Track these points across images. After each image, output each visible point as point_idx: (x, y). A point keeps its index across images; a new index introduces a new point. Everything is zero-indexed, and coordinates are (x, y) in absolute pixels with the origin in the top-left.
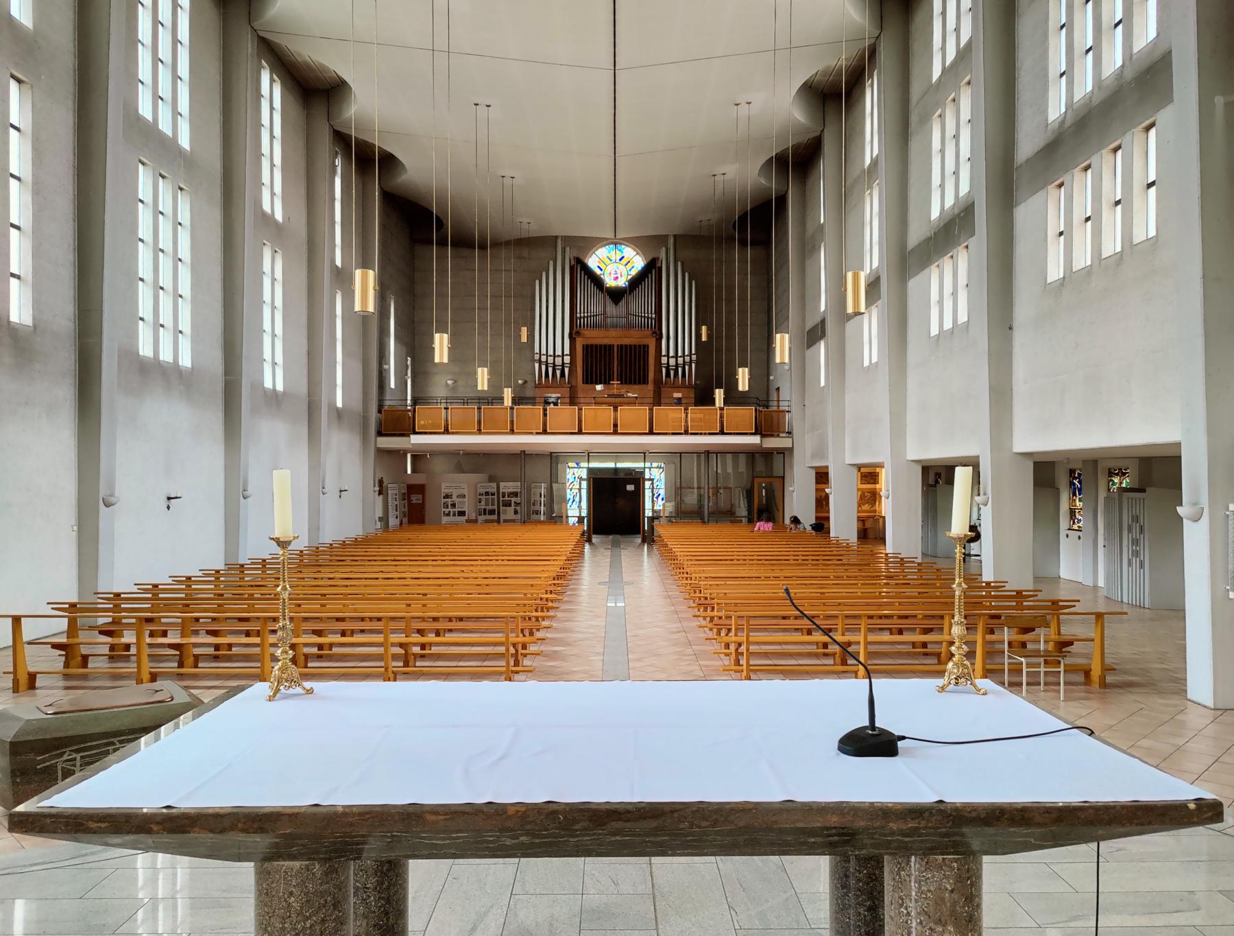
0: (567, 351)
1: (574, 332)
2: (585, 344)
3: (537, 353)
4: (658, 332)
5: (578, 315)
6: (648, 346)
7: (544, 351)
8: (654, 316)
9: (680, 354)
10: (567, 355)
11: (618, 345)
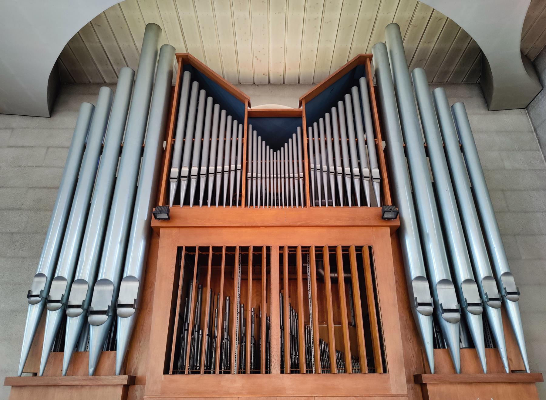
2: (185, 243)
3: (41, 275)
5: (175, 171)
6: (370, 248)
8: (376, 172)
11: (281, 248)
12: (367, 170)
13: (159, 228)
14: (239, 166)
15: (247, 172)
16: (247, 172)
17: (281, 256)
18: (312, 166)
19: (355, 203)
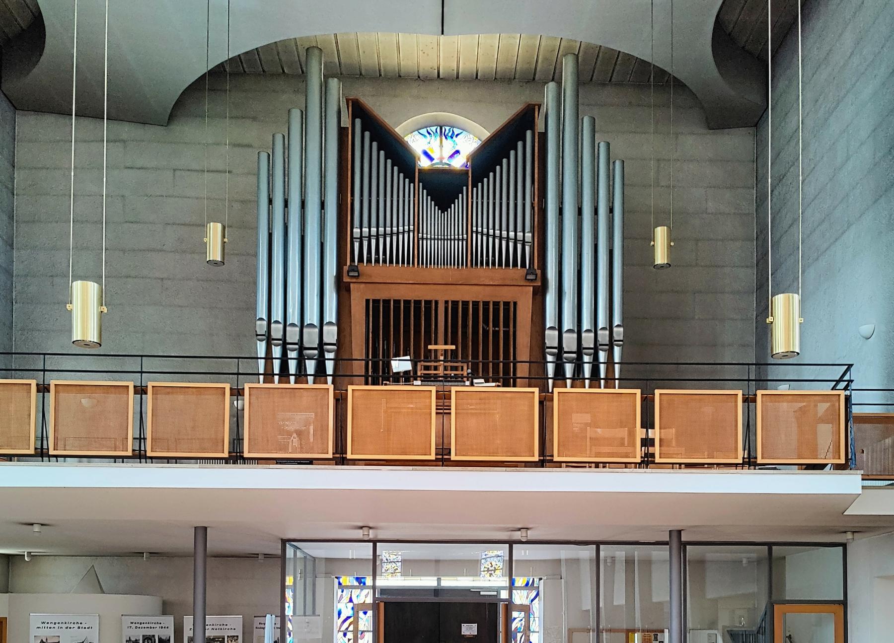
0: (331, 315)
1: (346, 268)
3: (261, 319)
4: (539, 272)
5: (357, 231)
6: (515, 304)
8: (528, 236)
10: (330, 323)
11: (446, 302)
12: (522, 234)
13: (350, 283)
14: (412, 227)
15: (418, 233)
16: (418, 233)
18: (474, 229)
19: (507, 265)
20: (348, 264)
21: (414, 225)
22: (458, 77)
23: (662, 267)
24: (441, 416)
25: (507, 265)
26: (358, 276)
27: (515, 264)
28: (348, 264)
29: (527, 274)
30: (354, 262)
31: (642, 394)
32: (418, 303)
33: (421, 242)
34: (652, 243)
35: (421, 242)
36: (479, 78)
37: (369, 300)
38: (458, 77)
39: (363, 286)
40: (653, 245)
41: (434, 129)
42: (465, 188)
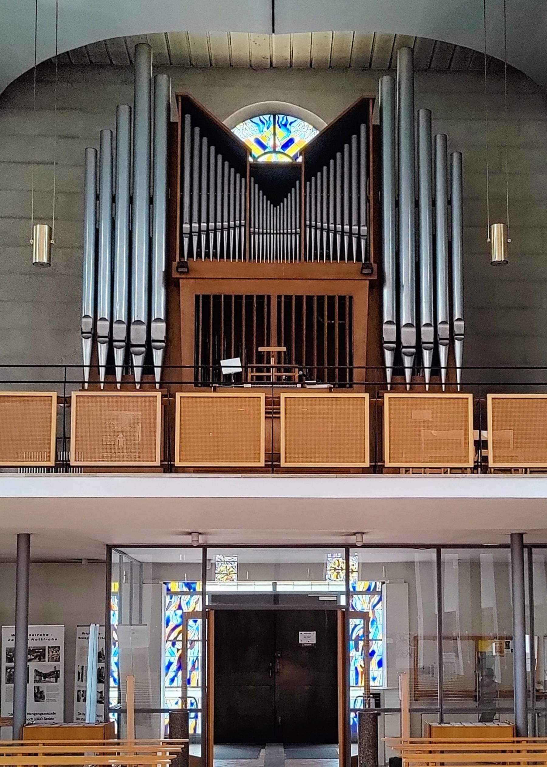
0: (159, 311)
1: (175, 264)
3: (87, 316)
4: (375, 266)
5: (186, 226)
6: (351, 298)
7: (104, 311)
8: (364, 229)
9: (425, 318)
10: (158, 320)
11: (279, 297)
12: (357, 227)
13: (179, 279)
14: (243, 222)
15: (250, 227)
16: (250, 227)
17: (279, 303)
18: (308, 223)
19: (342, 258)
20: (177, 259)
21: (245, 220)
22: (291, 66)
23: (499, 263)
24: (270, 420)
25: (342, 258)
26: (188, 271)
27: (350, 257)
28: (177, 259)
29: (362, 268)
30: (183, 257)
31: (474, 398)
32: (249, 298)
33: (252, 236)
34: (489, 240)
35: (252, 236)
36: (313, 66)
37: (199, 296)
38: (291, 66)
39: (192, 281)
40: (490, 242)
41: (267, 117)
42: (298, 182)
